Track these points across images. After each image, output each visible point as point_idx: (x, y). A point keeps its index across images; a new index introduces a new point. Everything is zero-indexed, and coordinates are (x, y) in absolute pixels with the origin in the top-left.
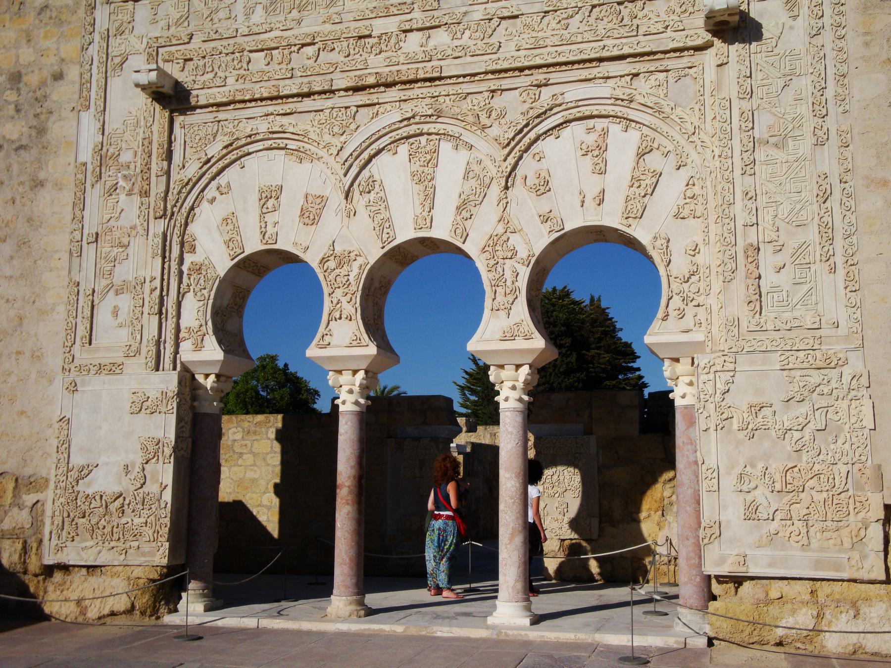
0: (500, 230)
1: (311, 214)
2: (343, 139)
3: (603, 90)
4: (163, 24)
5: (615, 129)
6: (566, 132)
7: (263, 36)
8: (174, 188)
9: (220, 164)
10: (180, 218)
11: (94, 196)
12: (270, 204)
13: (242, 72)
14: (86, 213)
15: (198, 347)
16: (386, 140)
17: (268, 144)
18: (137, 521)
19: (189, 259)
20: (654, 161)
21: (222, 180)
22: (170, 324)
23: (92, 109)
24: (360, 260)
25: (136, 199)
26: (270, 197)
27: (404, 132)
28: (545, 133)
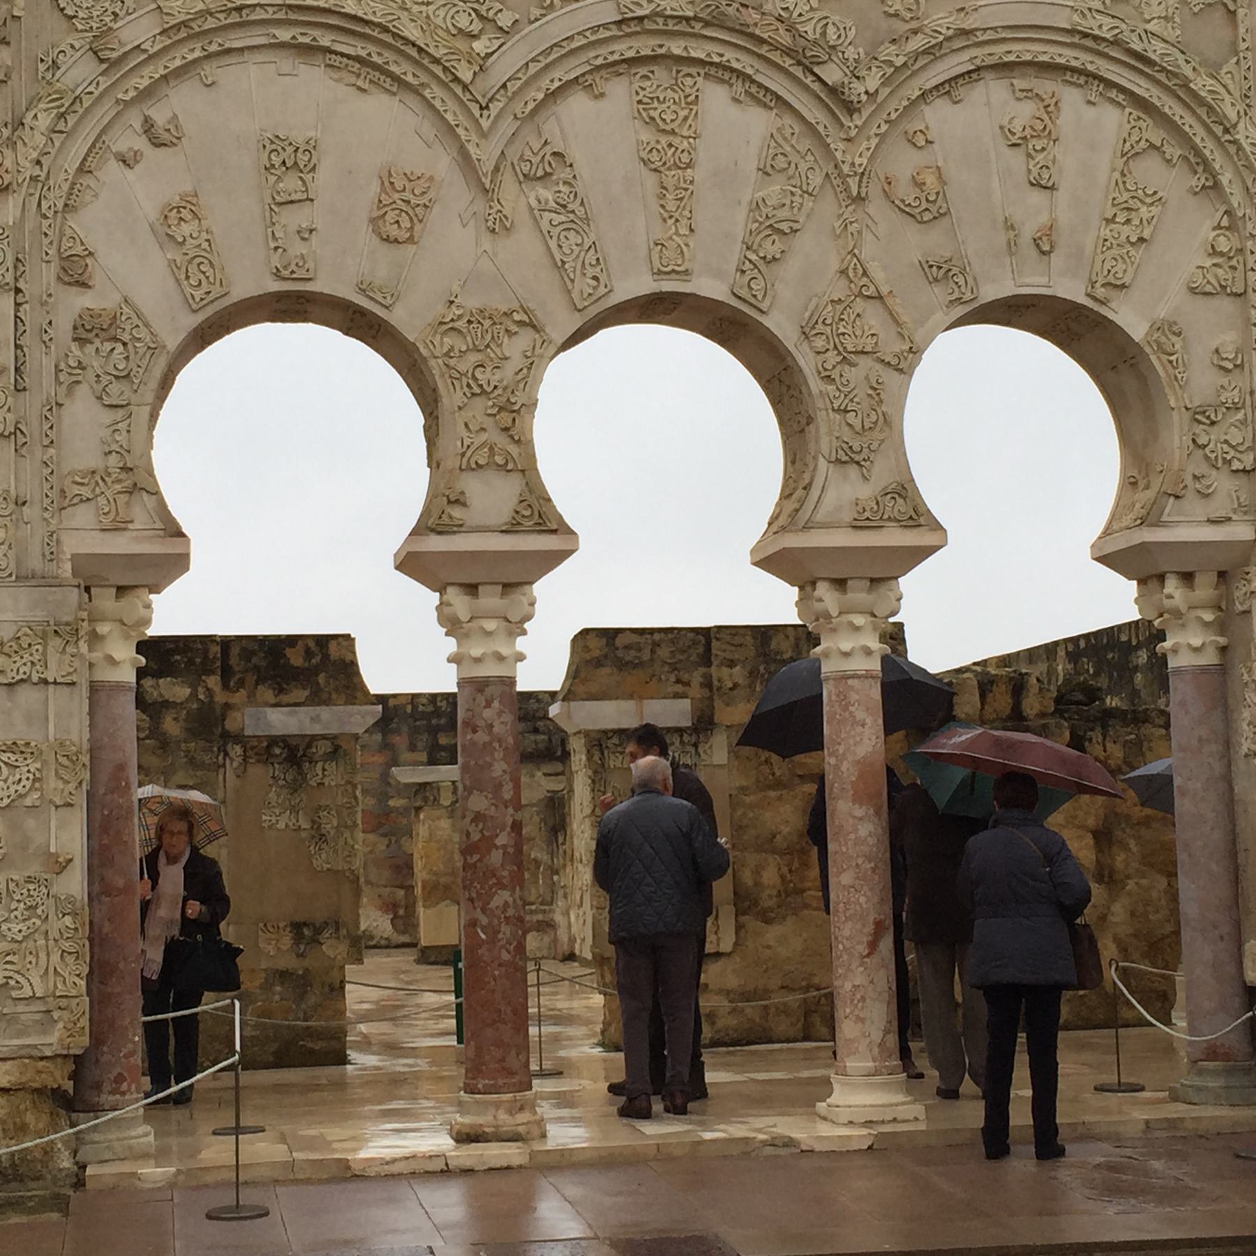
1: (399, 213)
2: (479, 46)
5: (1071, 98)
9: (156, 70)
17: (284, 35)
26: (289, 161)
27: (625, 49)
28: (936, 87)
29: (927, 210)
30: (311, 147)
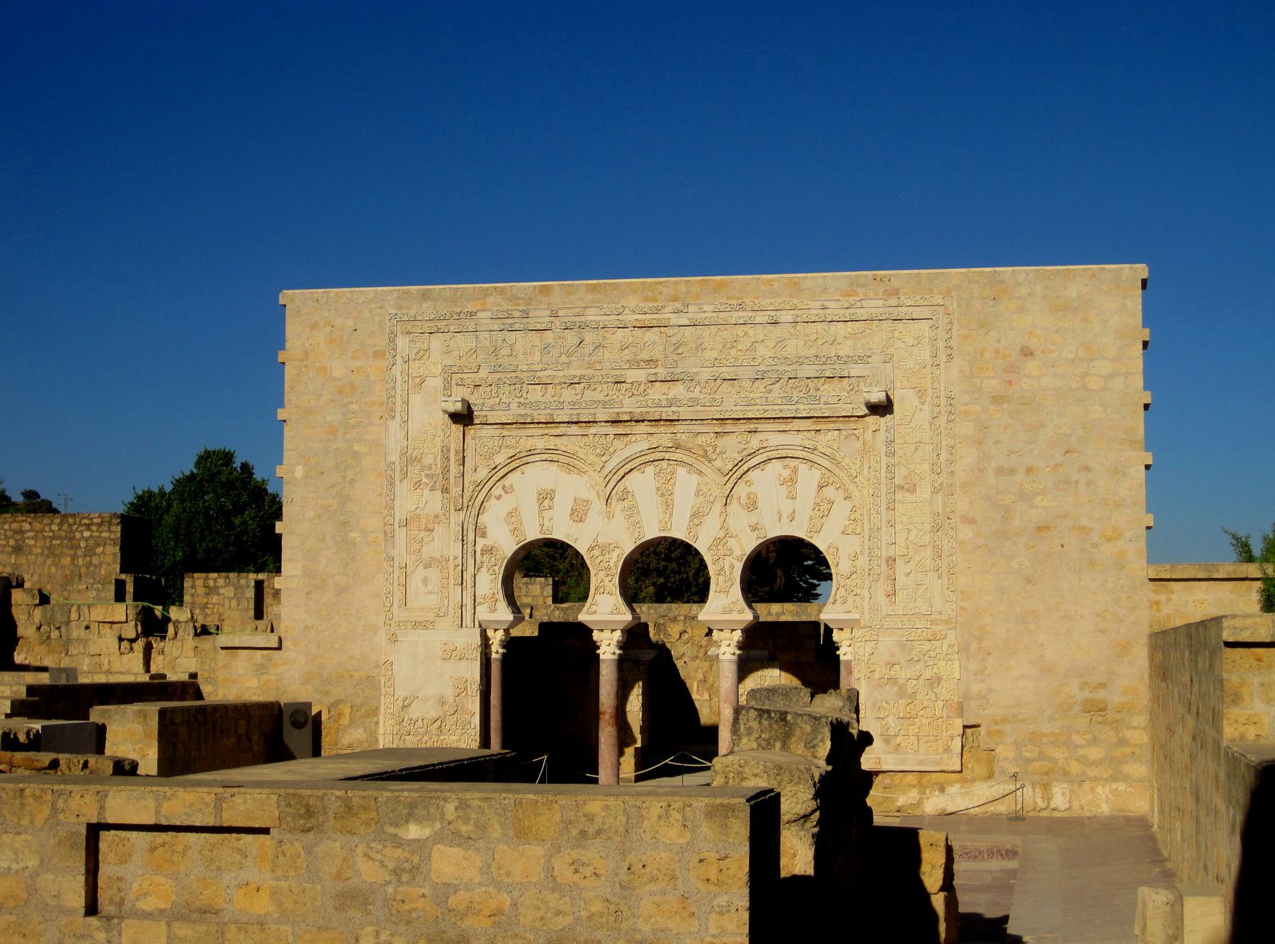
0: (722, 534)
1: (578, 514)
2: (604, 459)
3: (796, 439)
4: (456, 354)
5: (803, 467)
6: (769, 467)
7: (539, 374)
8: (469, 488)
10: (475, 511)
11: (402, 489)
12: (546, 503)
13: (522, 400)
14: (397, 503)
15: (493, 610)
16: (637, 462)
18: (453, 738)
19: (481, 543)
20: (829, 492)
21: (507, 482)
22: (470, 591)
23: (398, 419)
24: (617, 551)
25: (438, 493)
26: (546, 497)
29: (752, 505)
30: (553, 491)
